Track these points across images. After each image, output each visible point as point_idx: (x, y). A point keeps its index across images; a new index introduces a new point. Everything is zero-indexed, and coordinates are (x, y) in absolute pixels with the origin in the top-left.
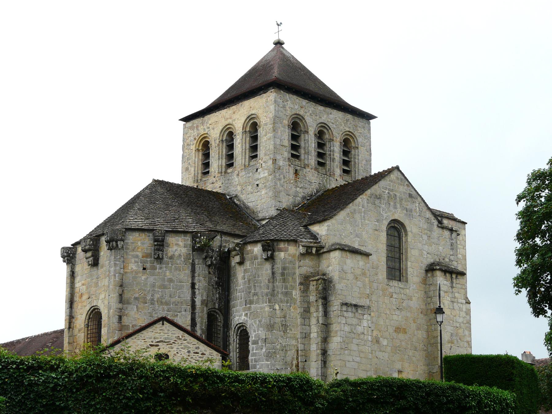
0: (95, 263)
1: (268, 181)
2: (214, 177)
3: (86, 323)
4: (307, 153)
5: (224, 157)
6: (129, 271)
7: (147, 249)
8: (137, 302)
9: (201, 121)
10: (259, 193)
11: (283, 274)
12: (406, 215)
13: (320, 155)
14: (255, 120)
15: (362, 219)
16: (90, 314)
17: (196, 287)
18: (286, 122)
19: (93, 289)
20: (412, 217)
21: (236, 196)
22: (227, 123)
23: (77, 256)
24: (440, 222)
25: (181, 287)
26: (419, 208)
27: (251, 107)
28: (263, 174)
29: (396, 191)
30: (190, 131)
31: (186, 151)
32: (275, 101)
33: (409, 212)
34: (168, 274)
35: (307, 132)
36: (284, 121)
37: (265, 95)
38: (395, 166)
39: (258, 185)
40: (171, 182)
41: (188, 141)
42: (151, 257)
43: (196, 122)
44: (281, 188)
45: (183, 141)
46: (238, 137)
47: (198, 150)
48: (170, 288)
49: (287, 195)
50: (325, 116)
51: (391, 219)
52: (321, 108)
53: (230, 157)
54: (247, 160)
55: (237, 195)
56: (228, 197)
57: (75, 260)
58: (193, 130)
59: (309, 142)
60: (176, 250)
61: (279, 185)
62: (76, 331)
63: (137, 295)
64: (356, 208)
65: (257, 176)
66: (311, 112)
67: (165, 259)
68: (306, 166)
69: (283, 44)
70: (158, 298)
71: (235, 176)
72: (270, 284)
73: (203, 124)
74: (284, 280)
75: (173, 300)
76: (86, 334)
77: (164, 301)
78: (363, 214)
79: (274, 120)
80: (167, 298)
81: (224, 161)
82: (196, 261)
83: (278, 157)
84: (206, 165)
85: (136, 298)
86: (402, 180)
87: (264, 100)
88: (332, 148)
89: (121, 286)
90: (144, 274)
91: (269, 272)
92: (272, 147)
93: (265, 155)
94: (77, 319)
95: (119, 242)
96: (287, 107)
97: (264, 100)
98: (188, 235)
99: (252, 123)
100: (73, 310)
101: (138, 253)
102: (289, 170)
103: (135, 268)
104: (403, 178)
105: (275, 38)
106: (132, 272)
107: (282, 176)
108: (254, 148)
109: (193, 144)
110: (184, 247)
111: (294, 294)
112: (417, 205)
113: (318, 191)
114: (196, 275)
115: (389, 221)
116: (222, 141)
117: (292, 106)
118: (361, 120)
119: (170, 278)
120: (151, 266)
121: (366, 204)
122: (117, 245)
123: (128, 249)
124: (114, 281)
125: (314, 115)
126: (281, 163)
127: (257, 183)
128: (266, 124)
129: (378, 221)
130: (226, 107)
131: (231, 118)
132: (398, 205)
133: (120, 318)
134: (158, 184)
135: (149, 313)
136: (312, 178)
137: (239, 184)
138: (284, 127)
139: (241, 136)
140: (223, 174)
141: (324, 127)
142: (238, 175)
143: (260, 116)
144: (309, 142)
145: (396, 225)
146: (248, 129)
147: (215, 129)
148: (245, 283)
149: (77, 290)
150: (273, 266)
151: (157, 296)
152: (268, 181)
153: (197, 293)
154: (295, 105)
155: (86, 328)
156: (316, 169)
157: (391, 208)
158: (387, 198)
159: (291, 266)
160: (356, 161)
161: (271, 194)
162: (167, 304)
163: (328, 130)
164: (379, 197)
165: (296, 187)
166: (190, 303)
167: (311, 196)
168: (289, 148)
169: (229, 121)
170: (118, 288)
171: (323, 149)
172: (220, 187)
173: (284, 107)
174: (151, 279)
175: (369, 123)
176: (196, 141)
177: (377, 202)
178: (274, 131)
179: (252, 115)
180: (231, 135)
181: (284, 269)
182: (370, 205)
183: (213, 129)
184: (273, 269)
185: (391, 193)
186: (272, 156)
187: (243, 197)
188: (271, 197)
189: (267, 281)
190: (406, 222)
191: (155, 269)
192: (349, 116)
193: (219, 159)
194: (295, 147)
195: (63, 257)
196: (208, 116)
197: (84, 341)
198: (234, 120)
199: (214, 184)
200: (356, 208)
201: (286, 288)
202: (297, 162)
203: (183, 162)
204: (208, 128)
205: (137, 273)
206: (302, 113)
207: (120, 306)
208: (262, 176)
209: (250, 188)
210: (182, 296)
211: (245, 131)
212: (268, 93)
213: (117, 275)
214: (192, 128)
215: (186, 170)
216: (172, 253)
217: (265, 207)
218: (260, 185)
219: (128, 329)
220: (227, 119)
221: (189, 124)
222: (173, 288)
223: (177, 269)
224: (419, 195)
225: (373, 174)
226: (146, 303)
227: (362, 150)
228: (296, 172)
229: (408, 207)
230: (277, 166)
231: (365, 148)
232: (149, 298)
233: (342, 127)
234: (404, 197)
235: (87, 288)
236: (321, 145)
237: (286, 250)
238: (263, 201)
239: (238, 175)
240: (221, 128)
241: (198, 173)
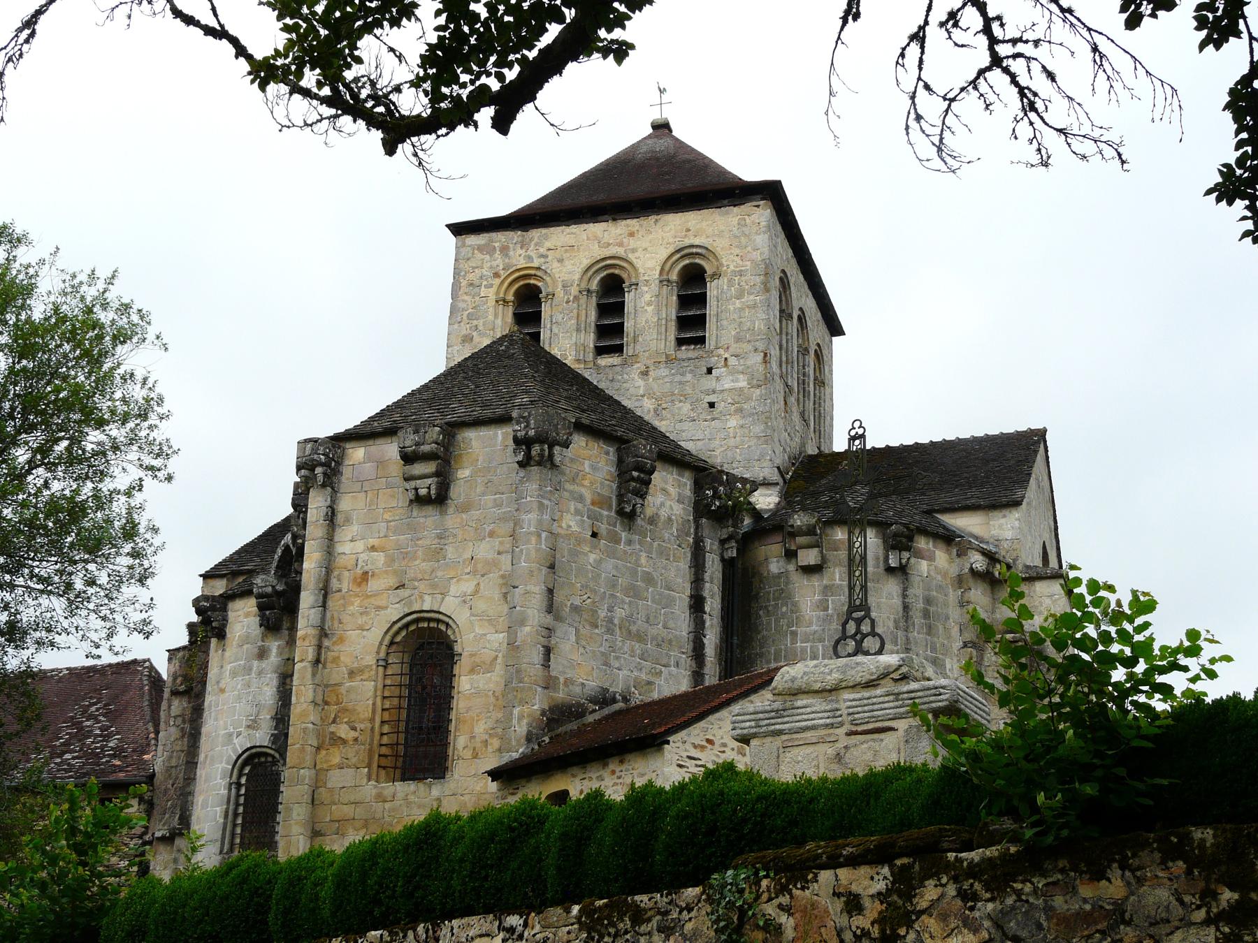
0: (439, 499)
3: (382, 655)
6: (563, 532)
7: (602, 484)
8: (577, 619)
11: (926, 615)
16: (397, 633)
17: (707, 609)
19: (420, 566)
23: (347, 472)
25: (669, 603)
27: (688, 230)
28: (728, 382)
30: (478, 255)
34: (643, 560)
37: (736, 209)
39: (712, 405)
42: (610, 508)
43: (500, 238)
48: (646, 599)
57: (339, 482)
60: (662, 504)
62: (336, 674)
63: (577, 602)
65: (709, 383)
67: (639, 521)
70: (622, 620)
72: (900, 633)
74: (930, 630)
75: (653, 631)
76: (380, 686)
77: (634, 628)
80: (640, 624)
82: (708, 543)
85: (575, 609)
87: (735, 220)
89: (552, 567)
90: (594, 547)
91: (897, 602)
93: (738, 339)
94: (342, 640)
95: (557, 449)
98: (687, 474)
100: (328, 615)
101: (583, 490)
103: (575, 528)
105: (656, 115)
106: (568, 537)
109: (491, 286)
110: (678, 501)
111: (948, 666)
114: (707, 577)
119: (648, 573)
120: (609, 532)
122: (551, 456)
123: (563, 473)
124: (538, 550)
127: (712, 398)
130: (601, 218)
131: (621, 244)
133: (548, 651)
135: (603, 654)
137: (649, 394)
142: (645, 373)
147: (567, 263)
148: (827, 620)
149: (341, 561)
150: (905, 589)
151: (619, 613)
153: (708, 624)
155: (381, 669)
159: (941, 597)
161: (758, 429)
162: (640, 637)
166: (689, 647)
169: (620, 251)
170: (544, 570)
174: (609, 565)
179: (693, 246)
181: (928, 601)
184: (904, 596)
186: (761, 346)
188: (759, 438)
189: (891, 624)
191: (618, 542)
193: (578, 330)
195: (305, 466)
196: (544, 231)
197: (374, 704)
198: (634, 251)
201: (934, 649)
205: (579, 541)
207: (548, 620)
208: (727, 386)
210: (671, 624)
212: (747, 208)
213: (544, 535)
214: (488, 249)
216: (654, 510)
217: (738, 458)
218: (720, 407)
219: (556, 689)
220: (609, 244)
221: (473, 240)
222: (653, 601)
223: (662, 552)
225: (868, 447)
226: (597, 627)
232: (602, 614)
235: (391, 560)
237: (931, 558)
238: (732, 442)
239: (645, 373)
240: (586, 262)
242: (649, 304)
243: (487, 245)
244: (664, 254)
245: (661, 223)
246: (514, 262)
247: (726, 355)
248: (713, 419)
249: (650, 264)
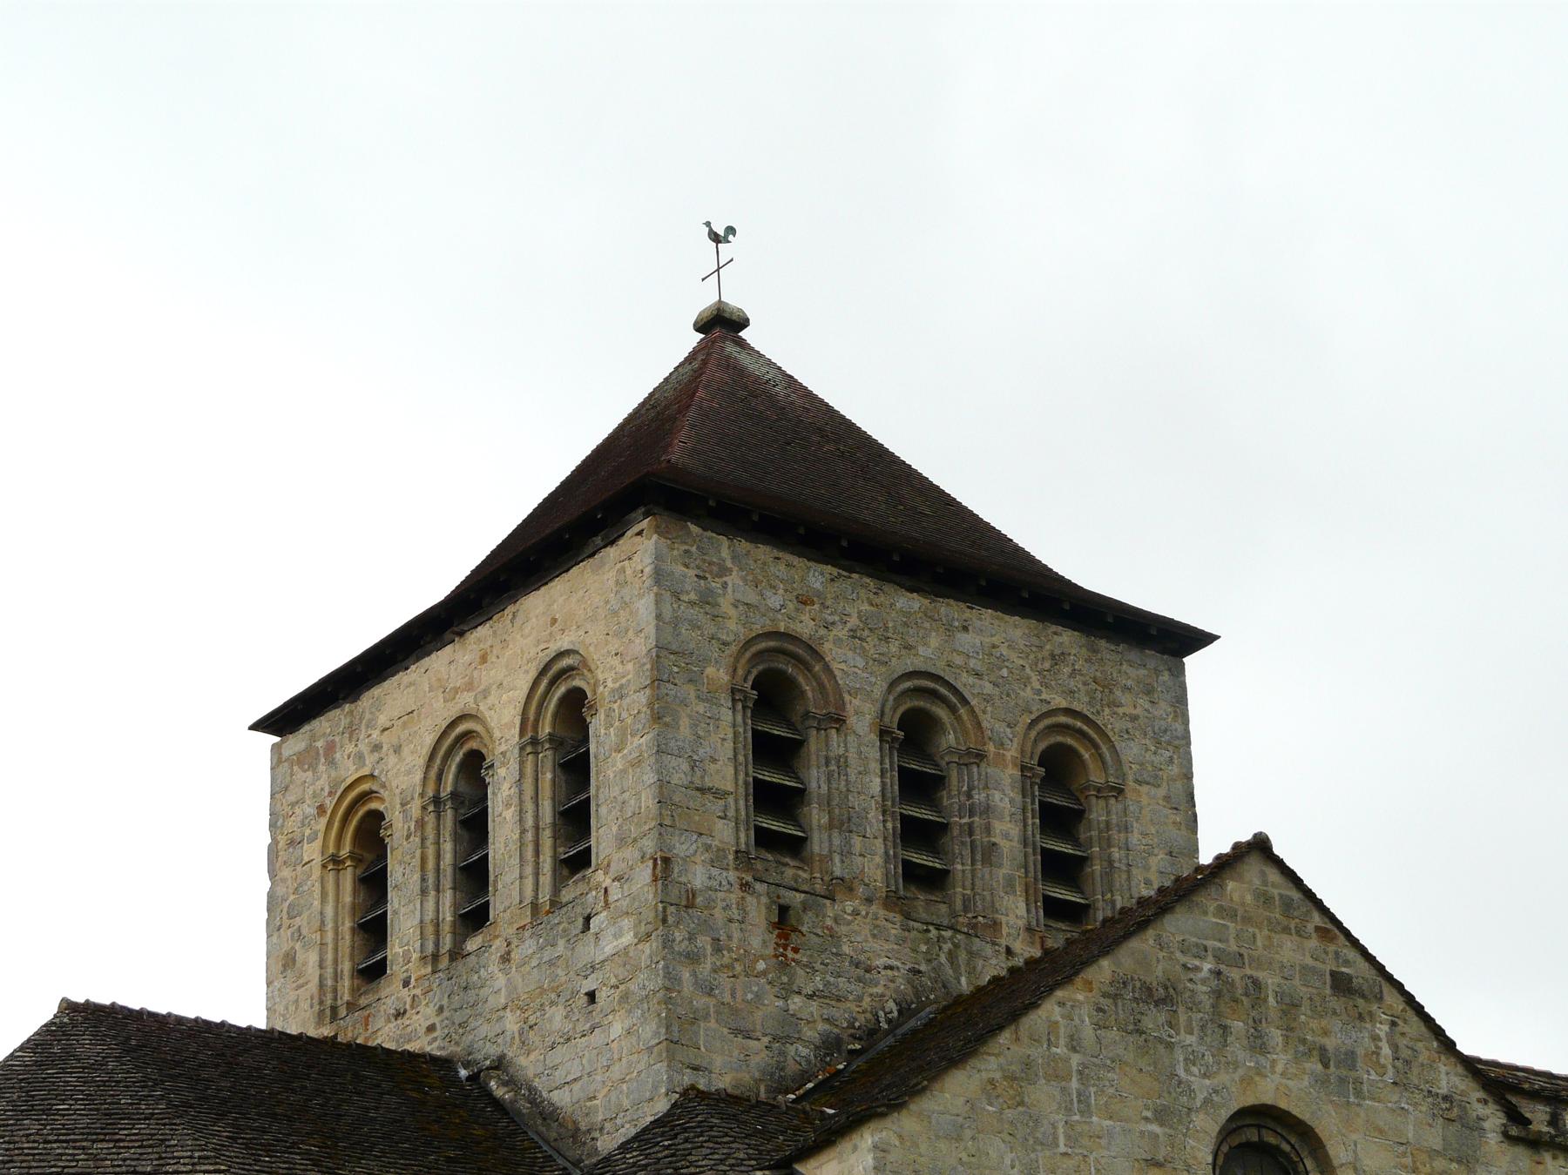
1: (637, 968)
2: (406, 983)
4: (844, 823)
5: (447, 882)
9: (344, 722)
10: (597, 1038)
12: (1322, 1082)
13: (916, 833)
14: (577, 683)
15: (1069, 1110)
18: (718, 674)
20: (1359, 1094)
21: (500, 1064)
22: (453, 711)
24: (1514, 1116)
26: (1395, 1048)
27: (554, 621)
28: (616, 937)
29: (1258, 963)
30: (301, 776)
31: (286, 873)
32: (659, 576)
33: (1338, 1069)
35: (838, 720)
36: (710, 671)
37: (611, 552)
38: (1246, 836)
40: (162, 1010)
41: (291, 824)
44: (701, 1001)
45: (273, 825)
46: (502, 772)
47: (336, 861)
49: (737, 1032)
50: (934, 641)
51: (1235, 1106)
52: (909, 603)
53: (474, 875)
54: (546, 879)
55: (501, 1058)
56: (463, 1073)
58: (313, 767)
59: (852, 771)
61: (687, 987)
64: (1037, 1053)
65: (588, 951)
66: (854, 621)
68: (838, 887)
69: (744, 323)
71: (494, 968)
73: (352, 731)
78: (1075, 1084)
79: (657, 663)
81: (448, 897)
83: (682, 847)
84: (374, 930)
86: (1287, 905)
87: (610, 576)
88: (979, 797)
92: (648, 801)
93: (621, 841)
96: (725, 605)
97: (610, 576)
99: (564, 700)
102: (741, 905)
104: (1296, 895)
105: (704, 300)
107: (704, 941)
108: (575, 819)
109: (311, 840)
112: (1383, 1030)
113: (905, 1011)
115: (1225, 1114)
116: (436, 800)
117: (752, 597)
118: (1134, 655)
121: (1088, 1032)
125: (866, 639)
126: (698, 876)
127: (588, 985)
128: (620, 693)
129: (1161, 1116)
130: (448, 635)
131: (470, 686)
132: (1276, 1036)
134: (80, 1019)
136: (876, 945)
137: (513, 1004)
138: (709, 698)
139: (514, 766)
140: (444, 962)
141: (933, 694)
142: (506, 958)
143: (595, 655)
144: (852, 771)
145: (1271, 1139)
146: (546, 729)
147: (406, 751)
152: (637, 968)
154: (763, 589)
156: (892, 901)
157: (1237, 1050)
158: (1207, 1002)
160: (1116, 854)
161: (650, 1031)
163: (953, 709)
164: (1164, 996)
165: (787, 992)
167: (872, 1033)
168: (740, 804)
169: (465, 701)
171: (934, 804)
172: (431, 1028)
173: (707, 600)
175: (1179, 671)
176: (324, 821)
177: (1154, 1019)
178: (657, 718)
180: (475, 765)
182: (1114, 1034)
183: (397, 750)
185: (1235, 974)
187: (528, 1065)
188: (650, 1049)
190: (1326, 1121)
192: (1066, 639)
193: (424, 892)
194: (770, 799)
196: (376, 691)
198: (486, 694)
199: (405, 1020)
200: (1037, 1053)
202: (791, 871)
203: (273, 928)
204: (377, 747)
206: (805, 626)
208: (609, 950)
209: (557, 1015)
211: (534, 742)
212: (627, 542)
214: (306, 759)
215: (282, 964)
217: (626, 1103)
218: (601, 996)
220: (456, 690)
221: (297, 742)
224: (1389, 978)
227: (1145, 802)
228: (783, 921)
229: (1330, 1043)
230: (674, 892)
231: (1162, 792)
233: (1028, 693)
234: (1303, 991)
236: (918, 785)
238: (617, 1071)
239: (506, 958)
240: (429, 739)
241: (337, 977)
242: (508, 806)
243: (309, 748)
244: (523, 683)
245: (520, 616)
246: (343, 773)
247: (608, 882)
248: (593, 1030)
249: (506, 719)
